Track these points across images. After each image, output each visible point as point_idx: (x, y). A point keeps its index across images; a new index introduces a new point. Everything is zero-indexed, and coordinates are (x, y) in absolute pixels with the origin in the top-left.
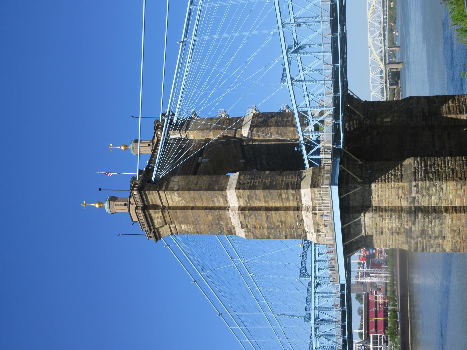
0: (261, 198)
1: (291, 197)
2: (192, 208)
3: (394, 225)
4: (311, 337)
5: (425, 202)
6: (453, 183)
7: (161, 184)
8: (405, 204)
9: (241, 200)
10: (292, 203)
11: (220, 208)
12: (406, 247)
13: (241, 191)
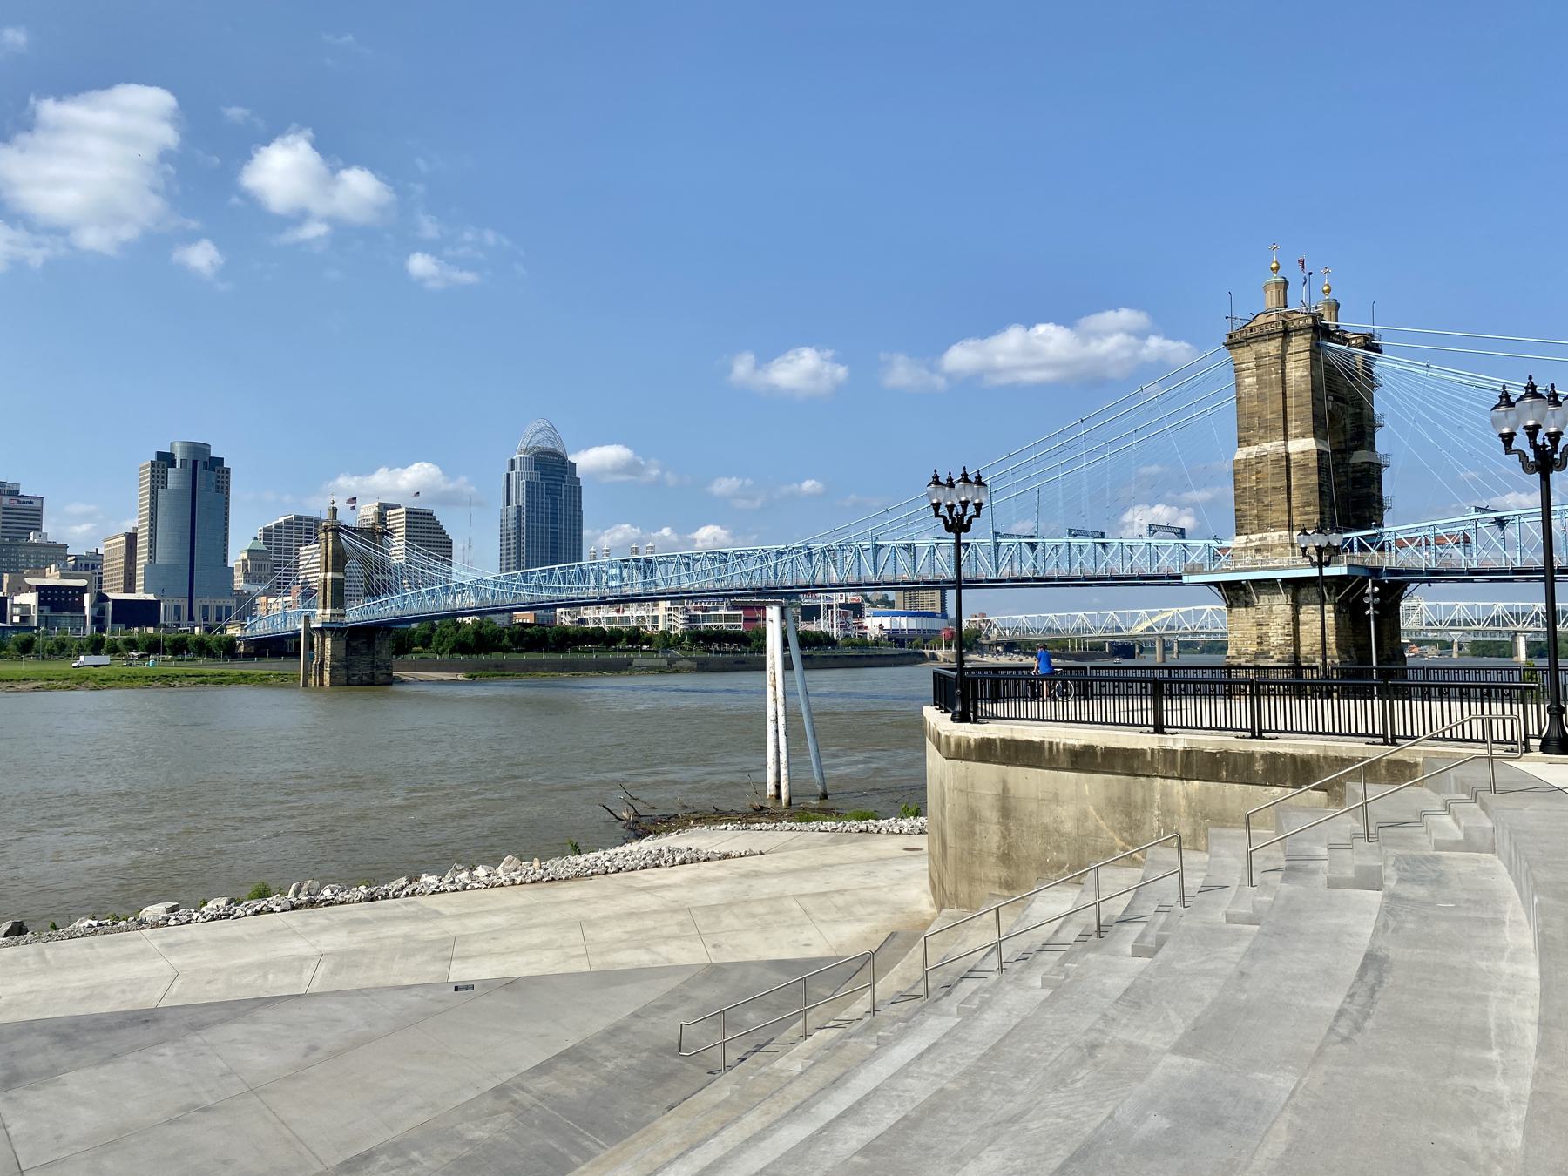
0: (1306, 482)
2: (1284, 394)
7: (1315, 353)
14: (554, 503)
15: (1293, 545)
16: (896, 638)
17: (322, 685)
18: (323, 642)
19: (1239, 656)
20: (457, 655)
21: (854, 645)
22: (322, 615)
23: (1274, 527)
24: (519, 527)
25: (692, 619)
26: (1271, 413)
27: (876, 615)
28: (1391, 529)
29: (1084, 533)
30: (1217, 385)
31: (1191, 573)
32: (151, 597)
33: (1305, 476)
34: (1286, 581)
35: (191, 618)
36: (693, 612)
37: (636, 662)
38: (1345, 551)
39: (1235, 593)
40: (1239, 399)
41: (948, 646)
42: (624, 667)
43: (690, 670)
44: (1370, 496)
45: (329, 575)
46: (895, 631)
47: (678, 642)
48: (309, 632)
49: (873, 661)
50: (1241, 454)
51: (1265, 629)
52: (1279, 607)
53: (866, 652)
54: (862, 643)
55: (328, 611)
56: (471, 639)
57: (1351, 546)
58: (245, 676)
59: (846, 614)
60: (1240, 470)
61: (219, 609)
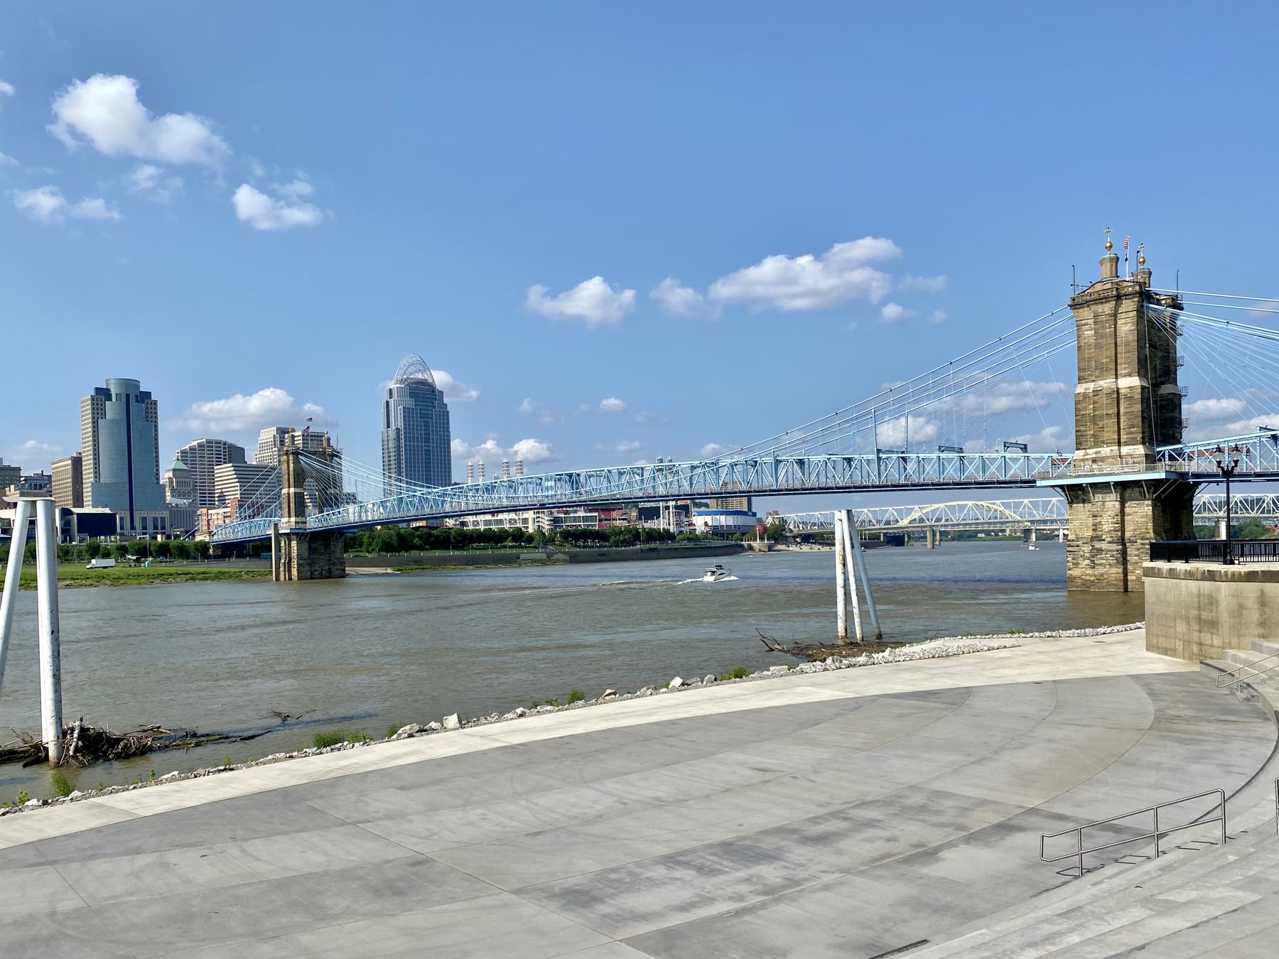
0: (1132, 411)
10: (1124, 438)
14: (427, 425)
16: (717, 532)
17: (290, 579)
20: (384, 554)
21: (689, 540)
22: (287, 523)
23: (1108, 444)
24: (399, 447)
25: (556, 521)
26: (1105, 358)
27: (700, 514)
28: (1192, 439)
29: (951, 449)
30: (1062, 335)
31: (1044, 479)
32: (107, 511)
33: (1131, 405)
34: (1117, 484)
35: (133, 527)
36: (556, 515)
37: (522, 556)
38: (1160, 460)
39: (1076, 493)
41: (762, 539)
42: (512, 561)
43: (565, 562)
44: (1173, 419)
45: (292, 490)
47: (551, 540)
48: (278, 536)
49: (706, 552)
53: (700, 544)
54: (692, 537)
56: (395, 540)
57: (1163, 456)
58: (223, 573)
59: (679, 514)
60: (1080, 400)
61: (155, 519)
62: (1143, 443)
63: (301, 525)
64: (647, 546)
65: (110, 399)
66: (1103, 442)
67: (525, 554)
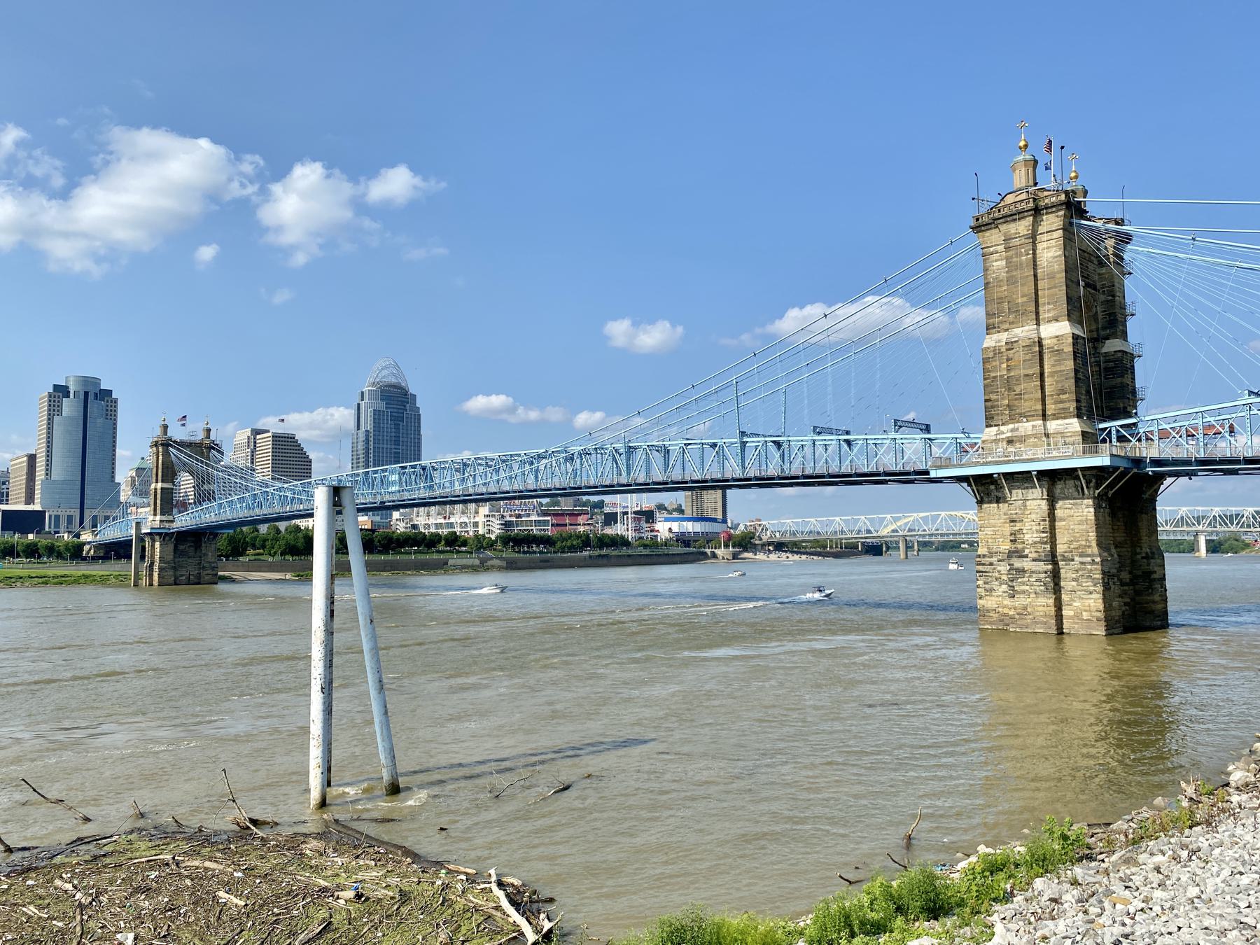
0: (1060, 369)
1: (1061, 406)
2: (1035, 276)
3: (1027, 536)
4: (764, 436)
5: (1066, 572)
6: (1101, 607)
8: (1061, 549)
9: (1055, 341)
10: (1051, 408)
11: (1037, 313)
12: (982, 550)
13: (1070, 340)
15: (1047, 436)
16: (683, 539)
18: (153, 546)
19: (991, 555)
21: (645, 546)
23: (1028, 416)
24: (367, 449)
25: (507, 524)
26: (1022, 296)
27: (667, 520)
28: (1149, 415)
29: (829, 431)
31: (940, 467)
34: (1042, 474)
36: (508, 519)
37: (451, 562)
38: (1104, 441)
39: (986, 488)
40: (987, 284)
41: (726, 546)
43: (500, 569)
44: (1123, 386)
45: (160, 485)
46: (683, 534)
47: (491, 545)
48: (141, 539)
49: (661, 560)
50: (990, 341)
51: (1018, 526)
52: (1034, 500)
53: (659, 551)
54: (653, 543)
55: (158, 518)
59: (639, 520)
62: (1079, 416)
63: (167, 525)
64: (598, 552)
65: (68, 397)
66: (1021, 415)
67: (454, 560)
